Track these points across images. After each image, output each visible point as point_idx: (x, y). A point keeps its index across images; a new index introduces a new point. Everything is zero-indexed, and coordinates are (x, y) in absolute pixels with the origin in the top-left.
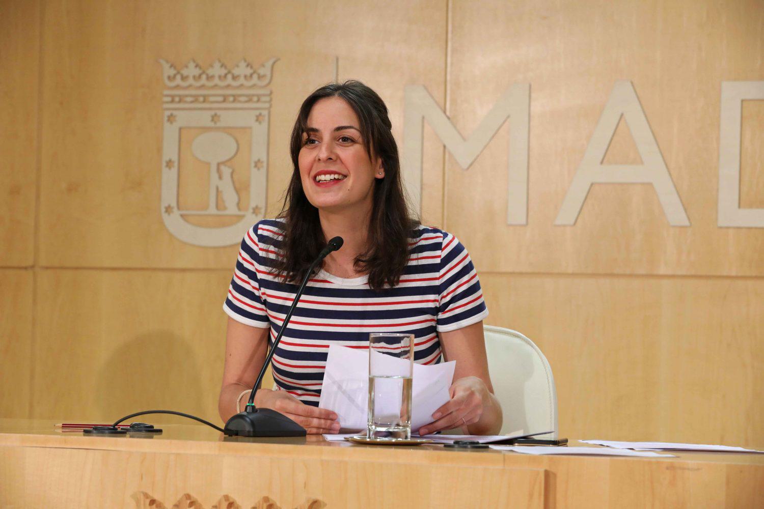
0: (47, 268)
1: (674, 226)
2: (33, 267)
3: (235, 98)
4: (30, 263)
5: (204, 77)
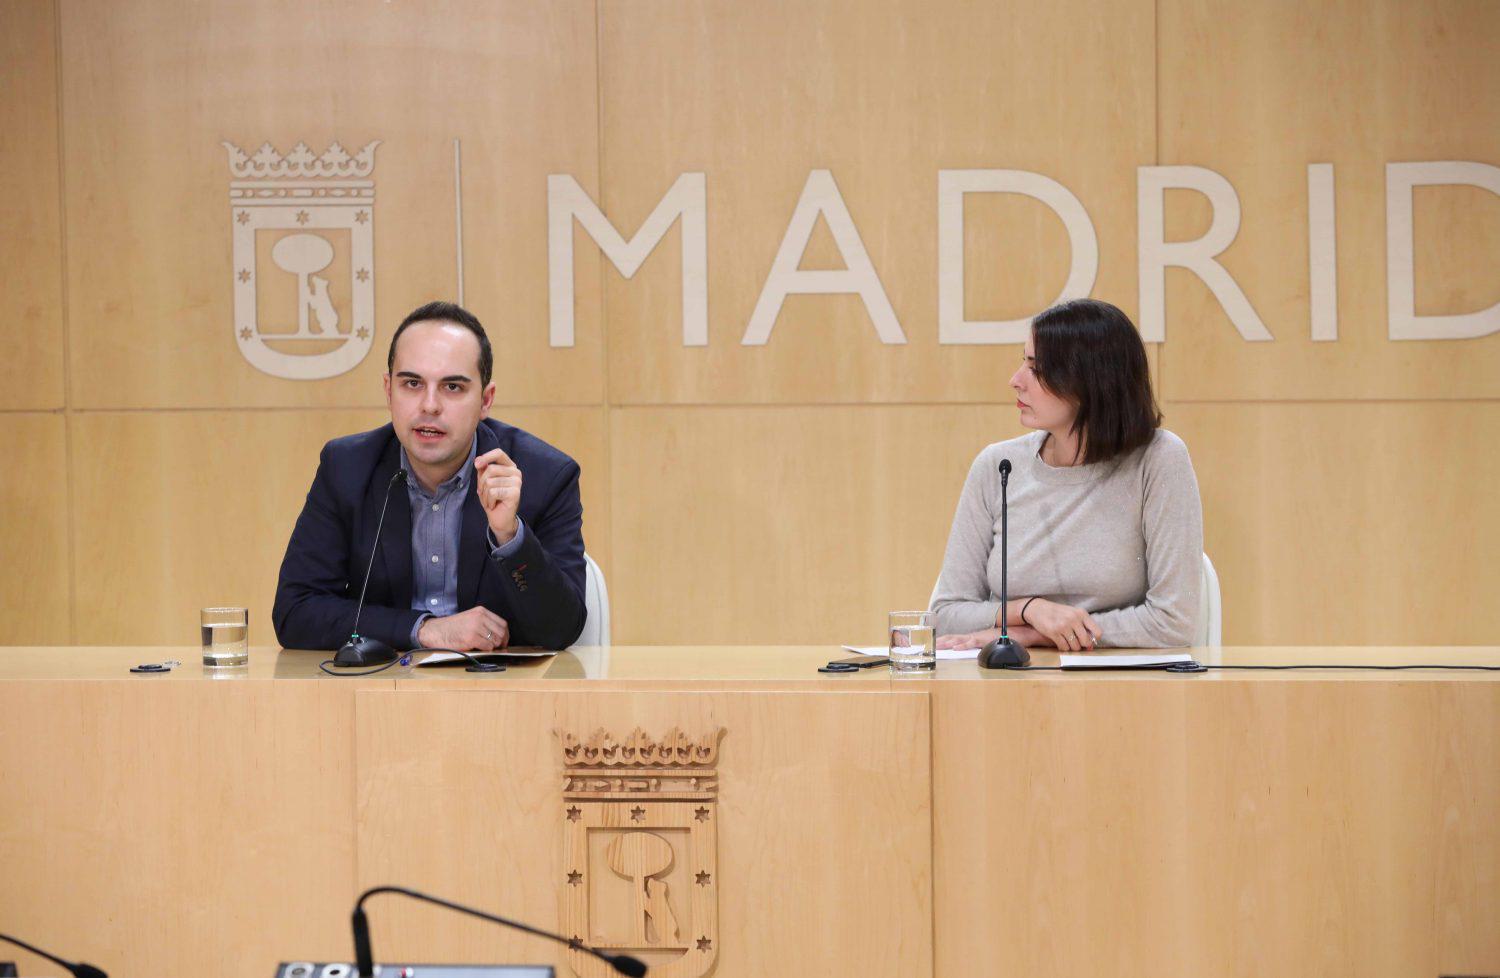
0: (82, 410)
1: (888, 345)
2: (62, 410)
3: (329, 192)
4: (62, 405)
5: (284, 165)
